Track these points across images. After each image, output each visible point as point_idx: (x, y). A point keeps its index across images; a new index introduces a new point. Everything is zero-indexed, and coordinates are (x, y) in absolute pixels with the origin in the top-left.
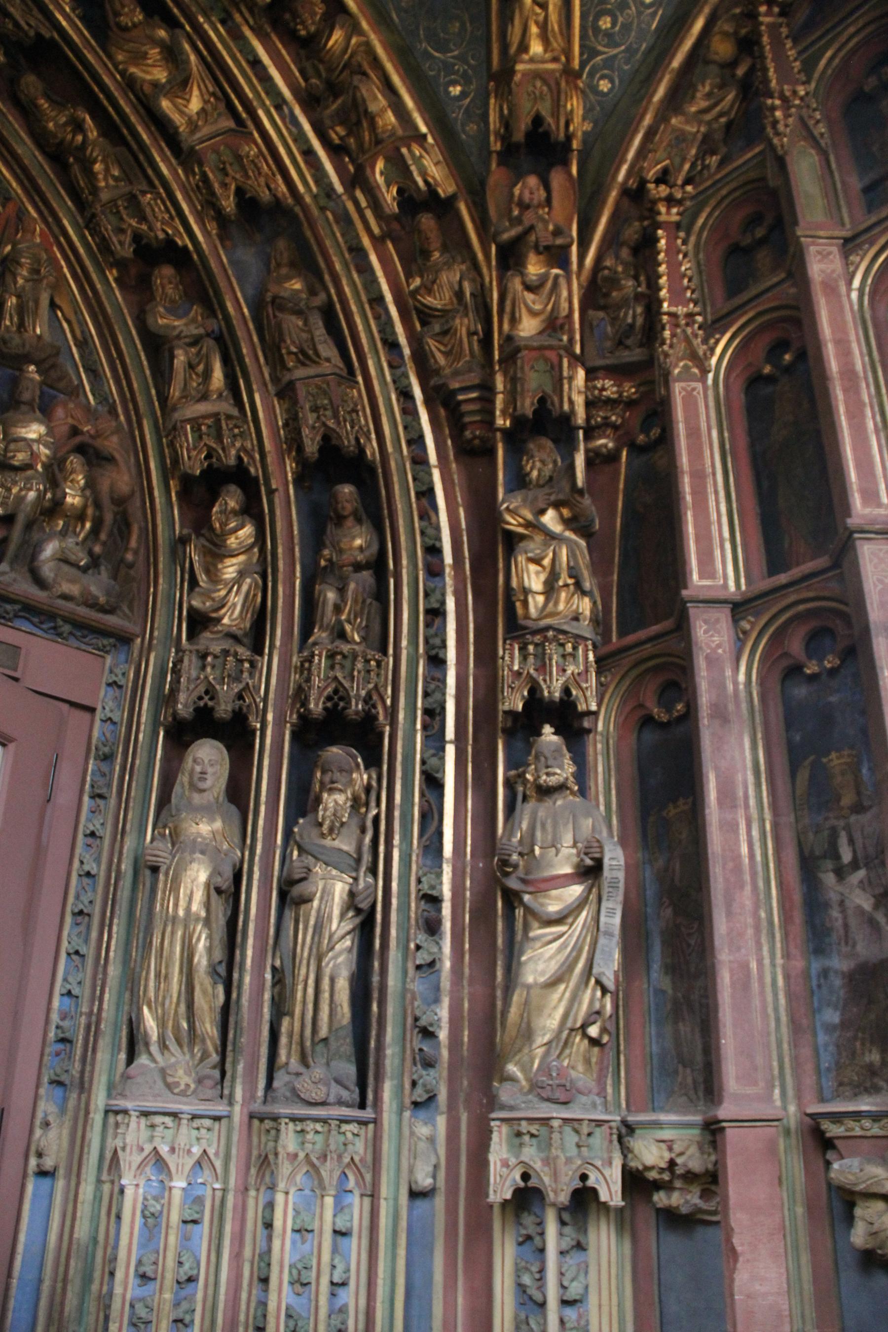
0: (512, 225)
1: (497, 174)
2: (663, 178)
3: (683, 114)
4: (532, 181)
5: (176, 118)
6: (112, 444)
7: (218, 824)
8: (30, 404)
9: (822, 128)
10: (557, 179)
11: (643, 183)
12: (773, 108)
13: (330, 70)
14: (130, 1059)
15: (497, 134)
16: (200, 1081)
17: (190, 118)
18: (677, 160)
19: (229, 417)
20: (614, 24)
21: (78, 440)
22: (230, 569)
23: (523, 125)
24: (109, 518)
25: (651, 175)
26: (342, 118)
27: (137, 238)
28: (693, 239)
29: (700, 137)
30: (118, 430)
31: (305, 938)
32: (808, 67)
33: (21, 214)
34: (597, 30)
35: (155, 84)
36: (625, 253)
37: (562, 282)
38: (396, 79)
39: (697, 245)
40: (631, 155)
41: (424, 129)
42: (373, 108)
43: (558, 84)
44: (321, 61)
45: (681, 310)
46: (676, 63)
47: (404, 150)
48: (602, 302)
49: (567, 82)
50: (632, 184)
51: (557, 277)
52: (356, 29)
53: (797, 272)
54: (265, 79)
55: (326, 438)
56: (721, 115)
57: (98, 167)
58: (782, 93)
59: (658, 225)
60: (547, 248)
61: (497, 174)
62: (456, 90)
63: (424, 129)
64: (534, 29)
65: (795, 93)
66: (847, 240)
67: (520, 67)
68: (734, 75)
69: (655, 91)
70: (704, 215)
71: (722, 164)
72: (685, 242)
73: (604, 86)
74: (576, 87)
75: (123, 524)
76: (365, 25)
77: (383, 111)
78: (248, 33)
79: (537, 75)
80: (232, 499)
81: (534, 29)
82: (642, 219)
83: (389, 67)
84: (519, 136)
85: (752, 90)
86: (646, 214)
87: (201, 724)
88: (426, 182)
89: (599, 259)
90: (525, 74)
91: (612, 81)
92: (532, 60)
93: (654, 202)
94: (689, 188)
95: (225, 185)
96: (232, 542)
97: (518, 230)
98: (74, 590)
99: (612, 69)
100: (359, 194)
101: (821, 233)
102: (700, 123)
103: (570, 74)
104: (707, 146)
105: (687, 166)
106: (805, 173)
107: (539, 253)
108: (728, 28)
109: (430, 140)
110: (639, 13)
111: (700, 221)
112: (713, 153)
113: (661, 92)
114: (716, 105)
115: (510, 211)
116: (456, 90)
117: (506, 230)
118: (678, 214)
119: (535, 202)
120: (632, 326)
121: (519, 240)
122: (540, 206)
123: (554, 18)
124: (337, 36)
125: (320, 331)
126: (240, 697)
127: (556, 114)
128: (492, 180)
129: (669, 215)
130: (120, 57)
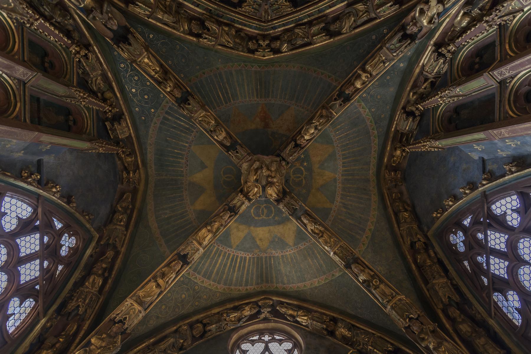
0: (107, 10)
1: (124, 22)
2: (86, 56)
3: (100, 75)
4: (115, 28)
9: (69, 100)
10: (111, 34)
11: (89, 51)
12: (84, 94)
13: (182, 17)
15: (135, 33)
18: (89, 64)
20: (134, 79)
23: (132, 40)
25: (90, 55)
26: (170, 7)
28: (60, 48)
29: (90, 74)
32: (88, 109)
34: (136, 75)
36: (70, 28)
37: (77, 4)
38: (166, 28)
39: (56, 47)
40: (99, 55)
41: (150, 20)
42: (166, 15)
43: (134, 57)
44: (185, 18)
45: (36, 23)
46: (114, 83)
47: (150, 10)
48: (59, 7)
49: (132, 59)
50: (91, 48)
51: (80, 4)
52: (183, 32)
53: (22, 63)
56: (92, 83)
58: (87, 99)
59: (73, 43)
60: (92, 11)
61: (124, 22)
62: (151, 36)
63: (150, 20)
64: (150, 64)
65: (84, 101)
66: (25, 84)
67: (146, 53)
68: (99, 92)
69: (111, 74)
70: (65, 56)
71: (78, 73)
72: (61, 45)
73: (122, 65)
74: (129, 60)
76: (182, 35)
77: (163, 17)
78: (204, 12)
79: (140, 55)
81: (150, 64)
82: (78, 41)
83: (170, 29)
84: (130, 36)
85: (93, 93)
86: (79, 44)
88: (138, 5)
89: (74, 20)
90: (143, 53)
91: (121, 68)
92: (144, 57)
93: (81, 49)
94: (77, 60)
97: (104, 11)
99: (125, 70)
101: (34, 79)
102: (94, 77)
103: (135, 61)
104: (85, 73)
105: (85, 64)
106: (59, 89)
107: (92, 7)
108: (112, 100)
109: (146, 18)
110: (132, 86)
111: (64, 54)
112: (82, 73)
113: (110, 75)
114: (96, 84)
115: (111, 14)
116: (151, 36)
117: (107, 8)
118: (72, 51)
119: (108, 22)
120: (42, 6)
121: (101, 7)
122: (106, 22)
123: (149, 70)
124: (186, 28)
127: (127, 49)
128: (124, 19)
129: (73, 49)
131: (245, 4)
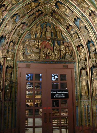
5: (67, 14)
6: (70, 45)
7: (86, 77)
8: (62, 44)
14: (82, 97)
16: (87, 98)
17: (68, 13)
19: (79, 40)
21: (67, 46)
22: (82, 54)
24: (71, 52)
27: (67, 26)
30: (70, 44)
31: (94, 86)
33: (56, 26)
35: (64, 11)
41: (90, 5)
42: (84, 6)
54: (73, 5)
55: (88, 40)
57: (61, 20)
75: (72, 52)
80: (81, 47)
87: (83, 69)
95: (73, 18)
96: (82, 51)
98: (70, 59)
100: (85, 13)
109: (91, 6)
125: (85, 29)
126: (85, 66)
130: (60, 9)
131: (55, 2)
